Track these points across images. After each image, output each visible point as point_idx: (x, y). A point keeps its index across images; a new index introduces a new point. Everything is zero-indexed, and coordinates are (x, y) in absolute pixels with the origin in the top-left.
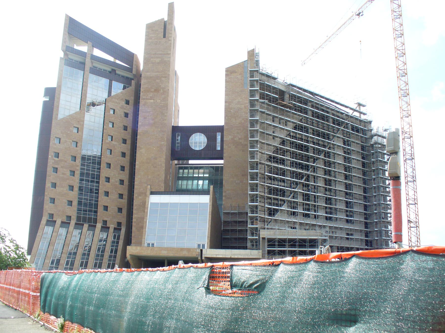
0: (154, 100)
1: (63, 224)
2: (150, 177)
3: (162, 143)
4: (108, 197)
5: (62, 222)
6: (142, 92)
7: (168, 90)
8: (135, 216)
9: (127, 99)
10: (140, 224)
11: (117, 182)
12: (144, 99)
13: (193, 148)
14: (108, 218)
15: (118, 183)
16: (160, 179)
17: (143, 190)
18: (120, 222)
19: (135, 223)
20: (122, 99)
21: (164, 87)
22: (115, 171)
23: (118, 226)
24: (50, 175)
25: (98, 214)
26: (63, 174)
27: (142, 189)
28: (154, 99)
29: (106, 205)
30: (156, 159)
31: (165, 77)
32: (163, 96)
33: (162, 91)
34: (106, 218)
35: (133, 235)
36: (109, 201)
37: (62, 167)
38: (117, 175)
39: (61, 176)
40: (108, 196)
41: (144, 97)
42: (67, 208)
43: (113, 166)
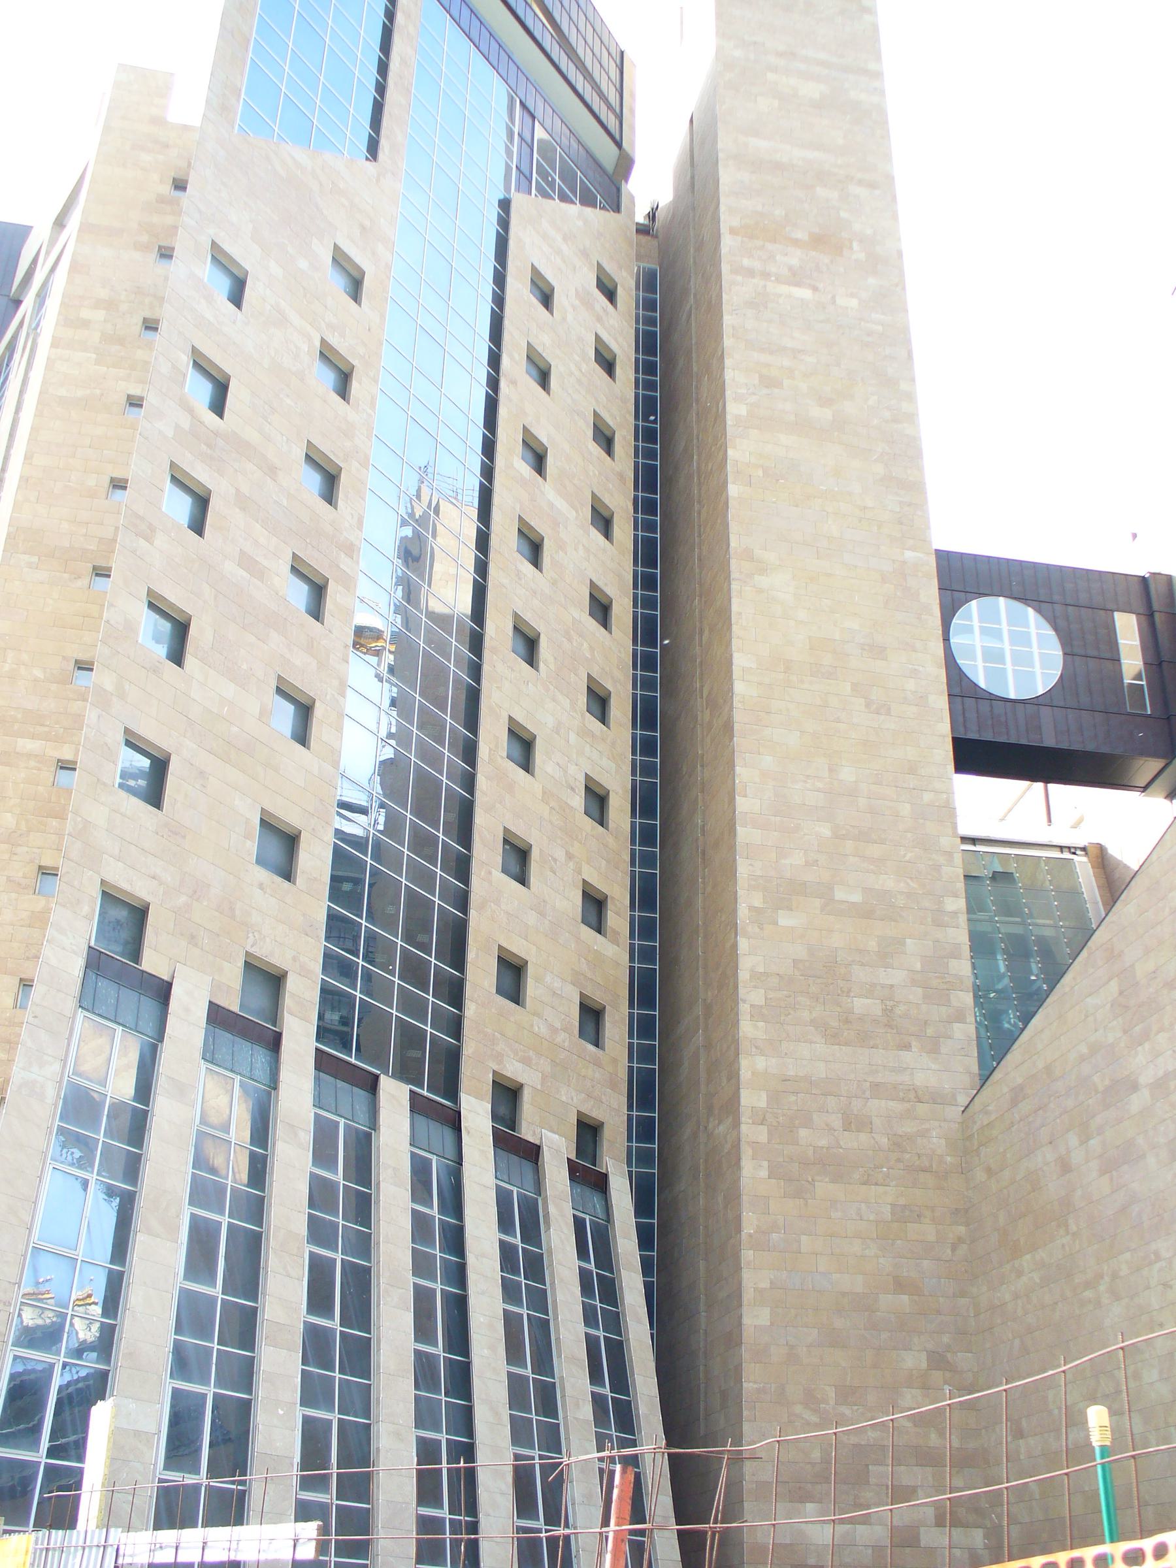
0: (815, 289)
1: (225, 1037)
2: (847, 774)
3: (909, 554)
4: (522, 879)
5: (218, 1016)
6: (733, 231)
7: (900, 254)
8: (761, 1063)
9: (610, 268)
10: (803, 1133)
11: (573, 789)
12: (750, 273)
13: (982, 685)
14: (526, 1061)
15: (578, 801)
16: (927, 797)
17: (807, 864)
18: (596, 1113)
19: (762, 1124)
20: (585, 254)
21: (869, 232)
22: (566, 703)
23: (578, 1155)
24: (152, 528)
25: (471, 1010)
26: (247, 562)
27: (797, 859)
28: (821, 286)
29: (518, 947)
30: (878, 651)
31: (872, 186)
32: (871, 280)
33: (858, 253)
34: (519, 1066)
35: (750, 1222)
36: (532, 918)
37: (242, 502)
38: (573, 737)
39: (231, 568)
40: (522, 879)
41: (746, 262)
42: (261, 886)
43: (551, 660)
